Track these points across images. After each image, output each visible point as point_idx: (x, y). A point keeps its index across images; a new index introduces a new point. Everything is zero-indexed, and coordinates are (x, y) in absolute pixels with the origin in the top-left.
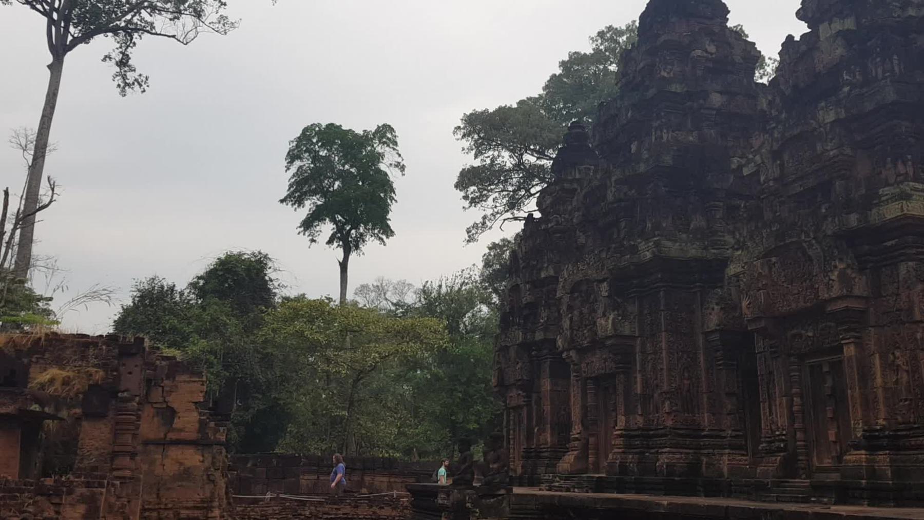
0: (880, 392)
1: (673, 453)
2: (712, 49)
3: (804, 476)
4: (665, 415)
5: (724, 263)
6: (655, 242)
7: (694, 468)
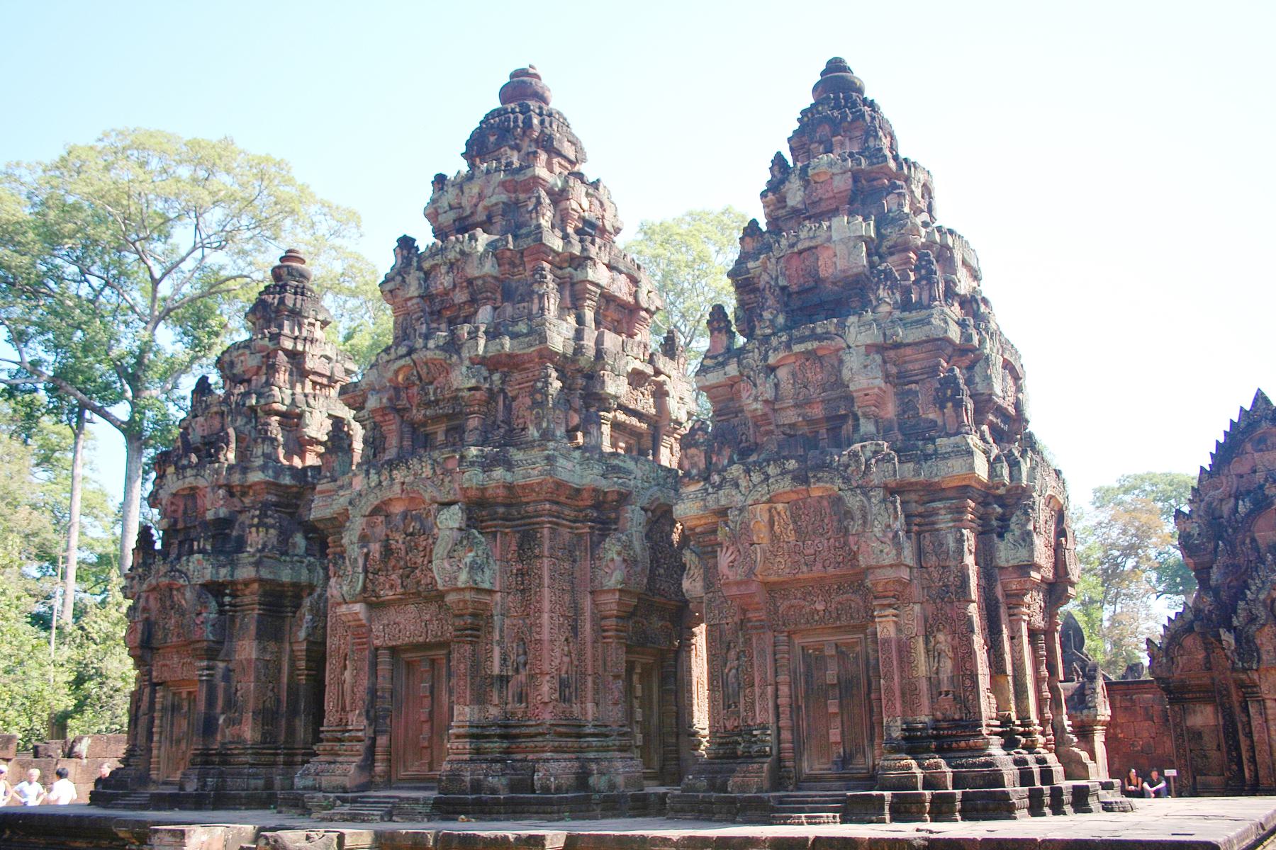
0: (924, 686)
1: (558, 760)
2: (586, 205)
3: (791, 787)
4: (541, 706)
5: (624, 498)
6: (548, 458)
7: (582, 779)
